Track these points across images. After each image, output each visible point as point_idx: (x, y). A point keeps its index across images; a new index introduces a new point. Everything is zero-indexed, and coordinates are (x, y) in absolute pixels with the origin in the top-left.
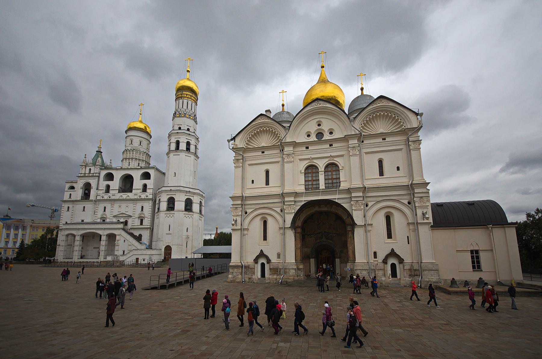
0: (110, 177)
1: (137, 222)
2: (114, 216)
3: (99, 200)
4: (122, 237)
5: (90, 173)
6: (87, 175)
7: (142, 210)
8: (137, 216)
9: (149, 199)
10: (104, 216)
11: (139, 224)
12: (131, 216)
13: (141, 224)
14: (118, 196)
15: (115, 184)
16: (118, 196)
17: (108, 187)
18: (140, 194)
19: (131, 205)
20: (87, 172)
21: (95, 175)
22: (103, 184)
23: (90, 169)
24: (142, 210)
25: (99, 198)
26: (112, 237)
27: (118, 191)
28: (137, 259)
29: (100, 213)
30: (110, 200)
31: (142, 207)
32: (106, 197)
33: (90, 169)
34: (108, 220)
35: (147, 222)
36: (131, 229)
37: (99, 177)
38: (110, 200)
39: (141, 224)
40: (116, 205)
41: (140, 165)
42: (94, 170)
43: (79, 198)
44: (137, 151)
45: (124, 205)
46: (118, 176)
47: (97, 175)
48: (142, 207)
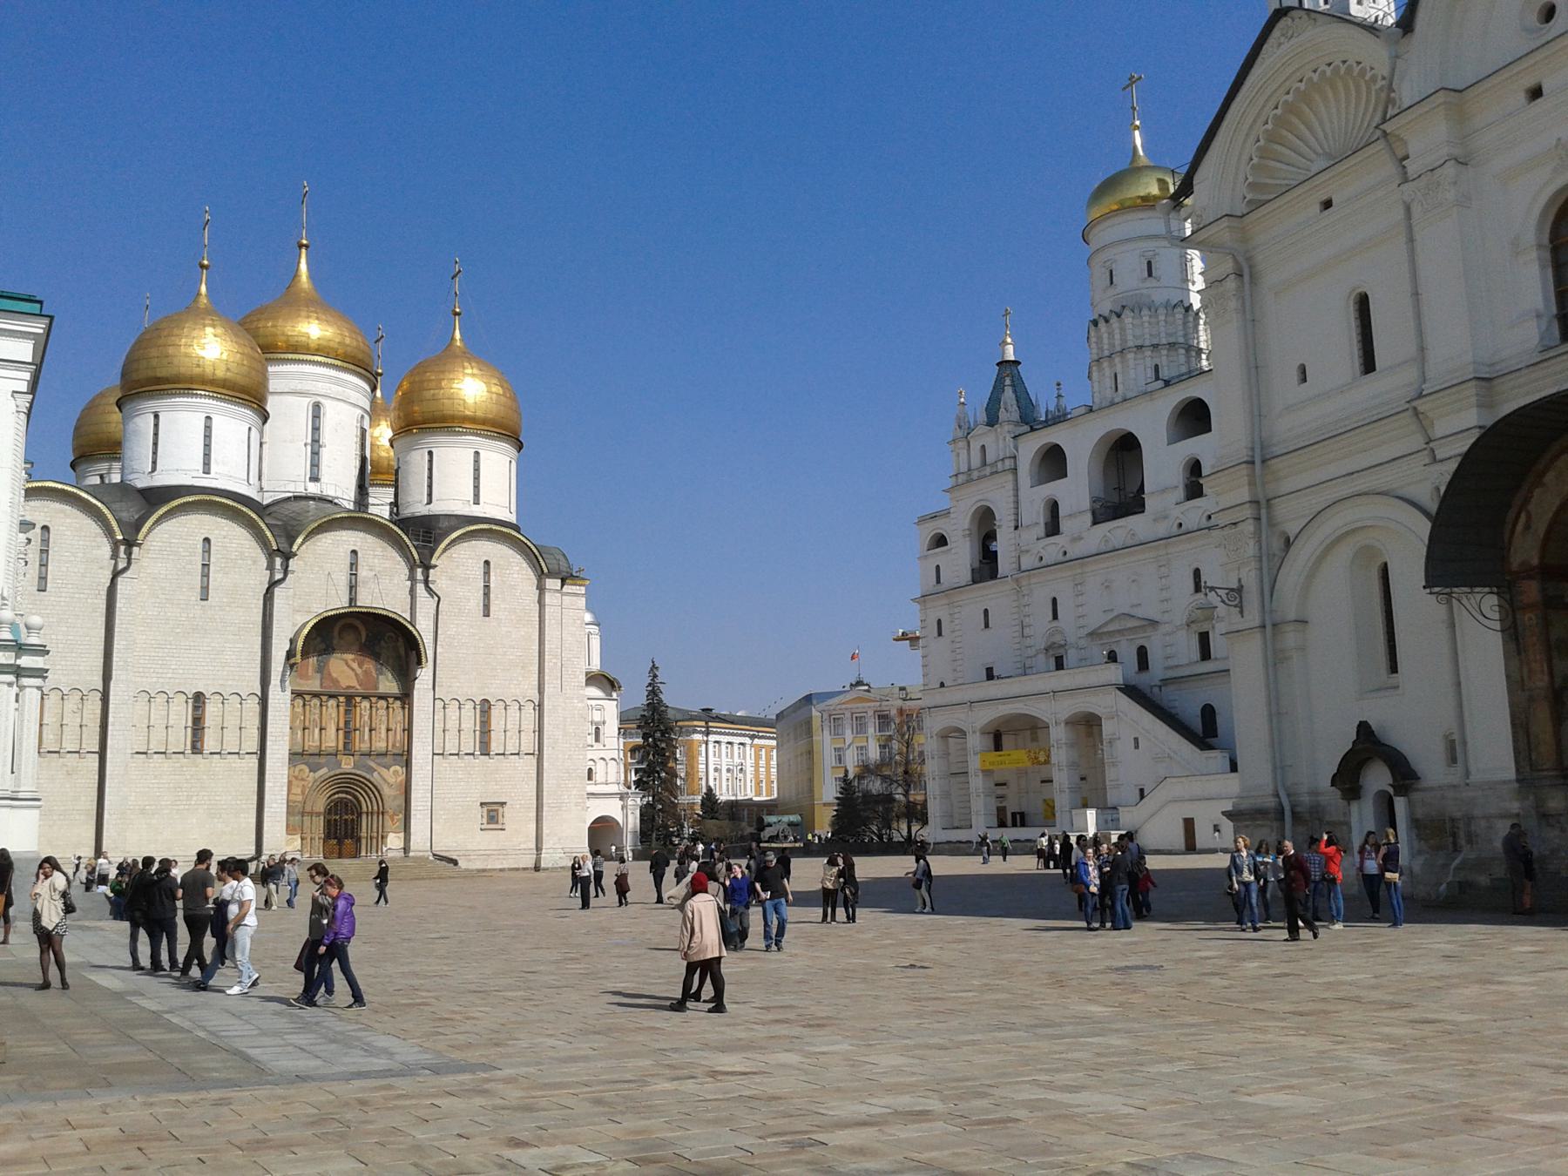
0: (1053, 462)
2: (1091, 634)
4: (1129, 725)
5: (984, 463)
8: (1180, 617)
10: (1058, 639)
11: (1196, 655)
12: (1154, 623)
15: (1077, 489)
17: (1054, 508)
20: (976, 461)
22: (1034, 499)
26: (1088, 725)
27: (1088, 518)
28: (1189, 824)
34: (1071, 657)
36: (1166, 682)
37: (1015, 470)
38: (1066, 560)
39: (1205, 654)
41: (1165, 373)
42: (996, 442)
44: (1137, 308)
46: (1082, 445)
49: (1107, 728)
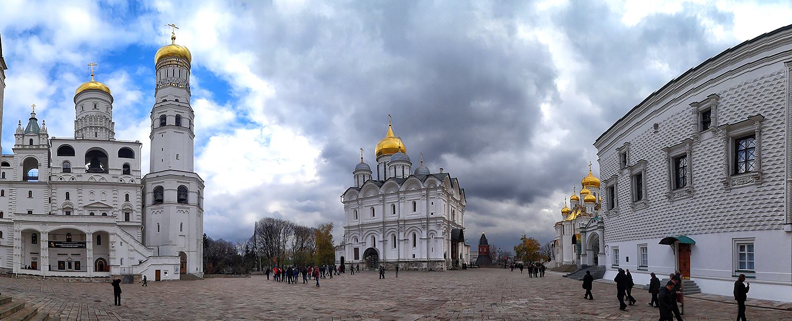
1: (121, 217)
3: (57, 183)
6: (28, 147)
7: (127, 199)
9: (136, 186)
12: (111, 208)
13: (127, 219)
14: (87, 177)
16: (87, 177)
18: (121, 177)
19: (109, 192)
21: (41, 147)
23: (31, 141)
24: (127, 199)
25: (54, 179)
29: (60, 200)
30: (73, 183)
31: (127, 196)
32: (67, 178)
33: (31, 141)
35: (135, 218)
38: (73, 183)
40: (86, 191)
43: (20, 178)
45: (98, 191)
47: (46, 147)
48: (127, 196)
49: (112, 238)
